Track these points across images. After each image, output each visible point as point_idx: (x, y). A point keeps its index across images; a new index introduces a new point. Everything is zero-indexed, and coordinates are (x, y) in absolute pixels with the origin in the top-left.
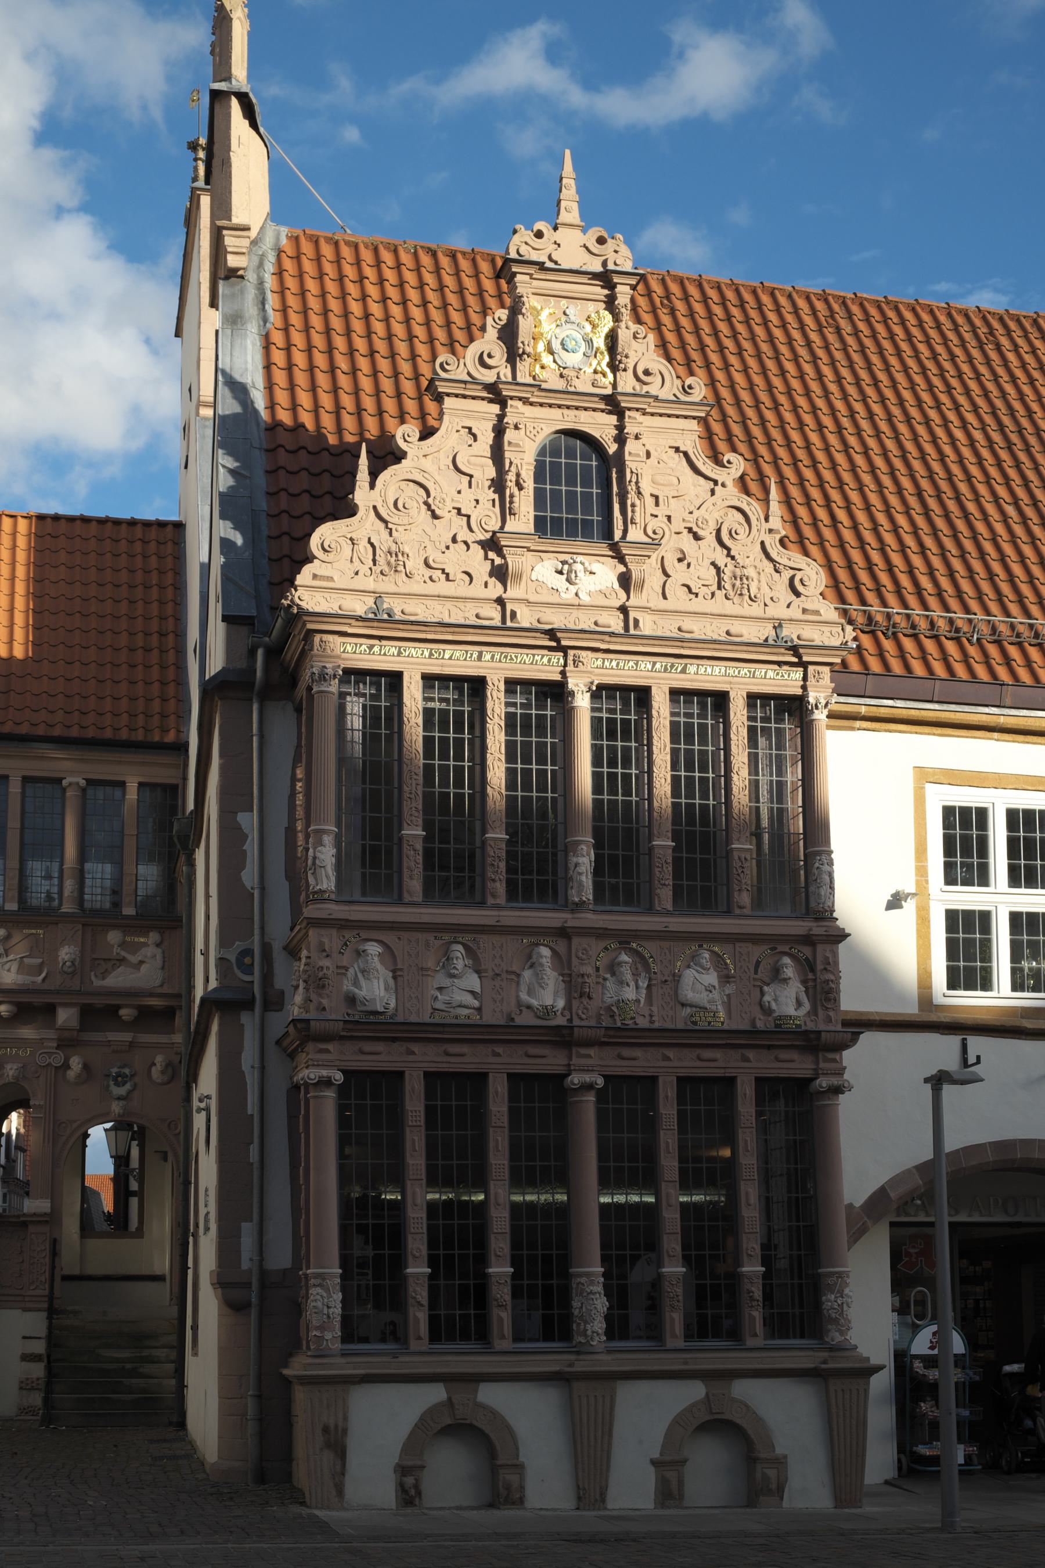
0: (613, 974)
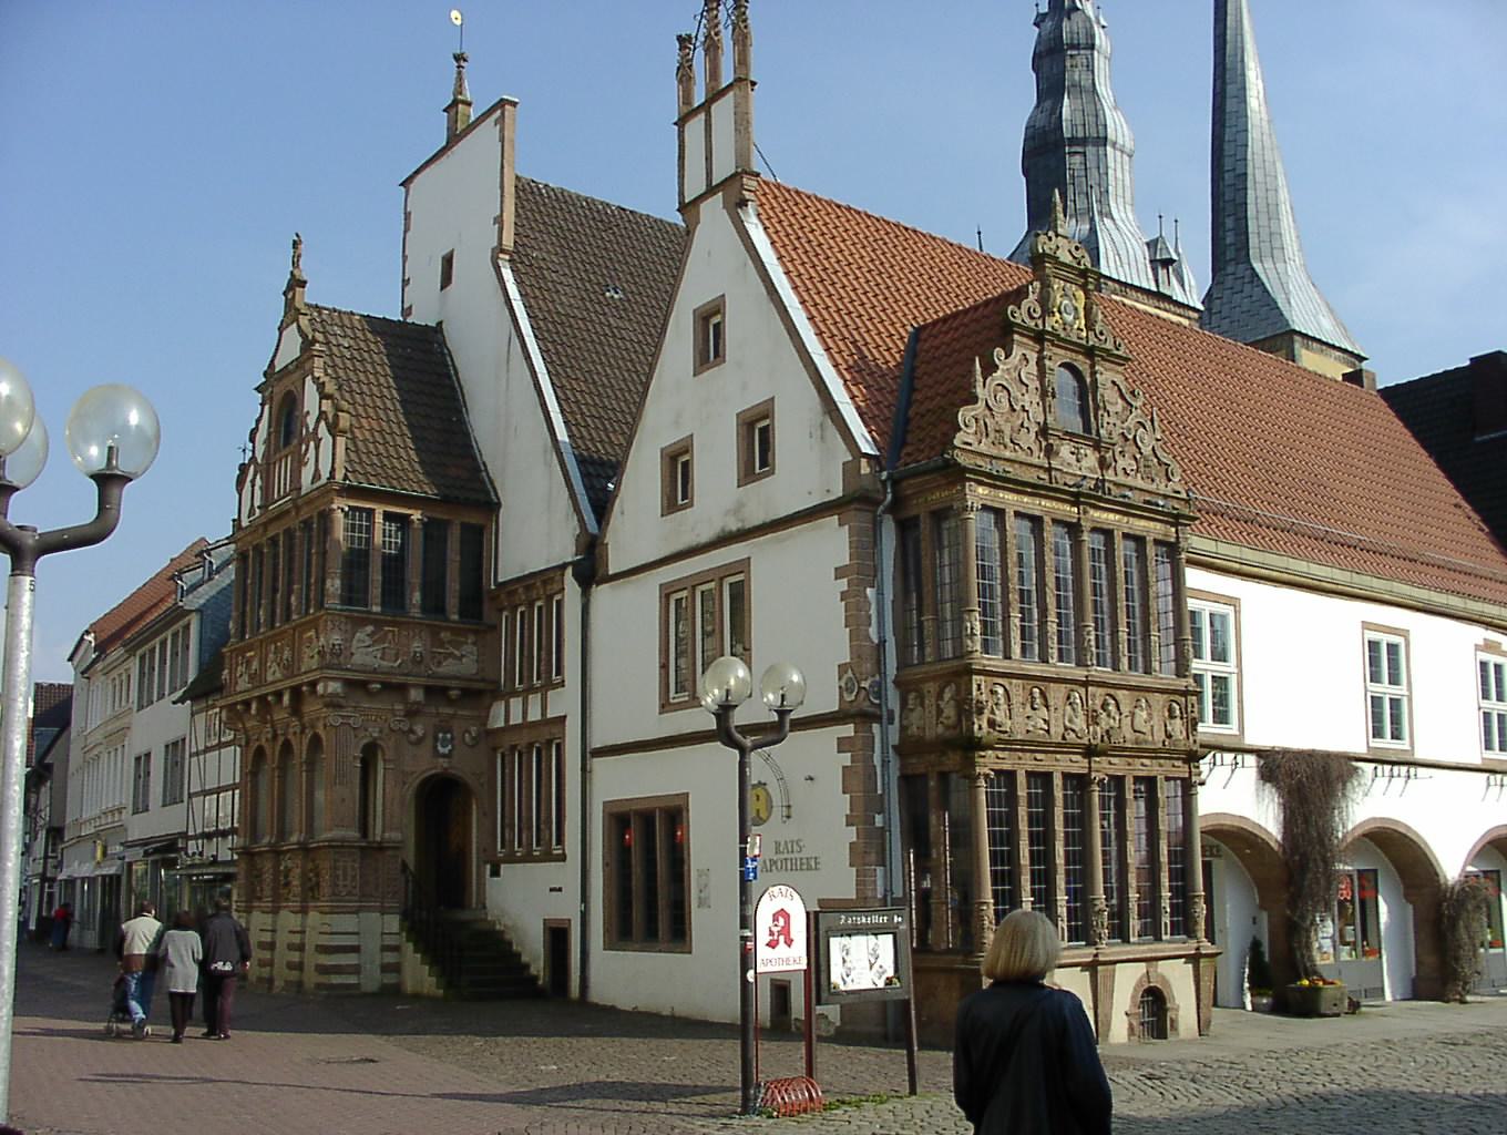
0: (1105, 711)
